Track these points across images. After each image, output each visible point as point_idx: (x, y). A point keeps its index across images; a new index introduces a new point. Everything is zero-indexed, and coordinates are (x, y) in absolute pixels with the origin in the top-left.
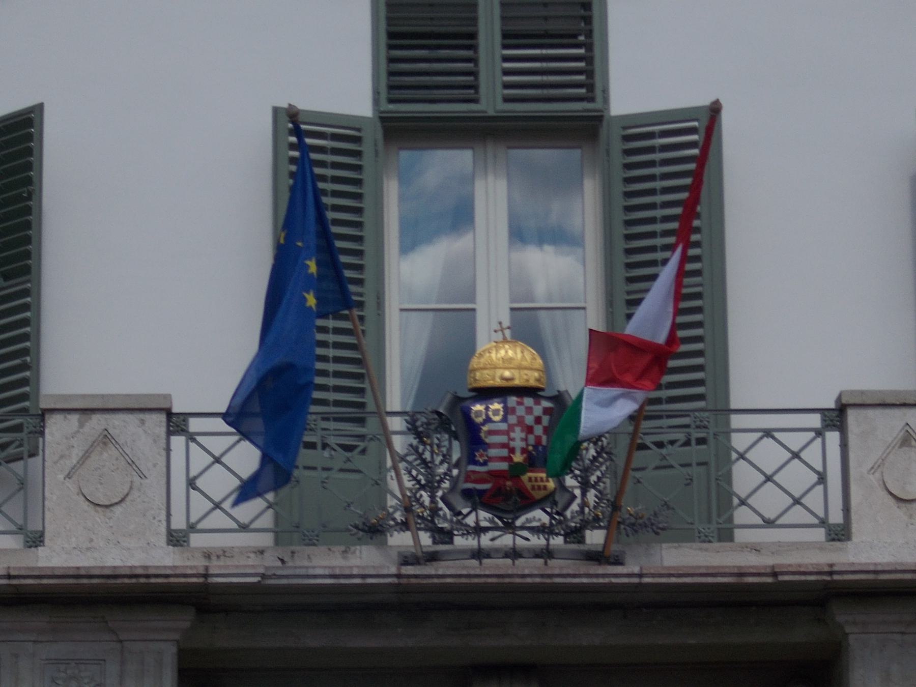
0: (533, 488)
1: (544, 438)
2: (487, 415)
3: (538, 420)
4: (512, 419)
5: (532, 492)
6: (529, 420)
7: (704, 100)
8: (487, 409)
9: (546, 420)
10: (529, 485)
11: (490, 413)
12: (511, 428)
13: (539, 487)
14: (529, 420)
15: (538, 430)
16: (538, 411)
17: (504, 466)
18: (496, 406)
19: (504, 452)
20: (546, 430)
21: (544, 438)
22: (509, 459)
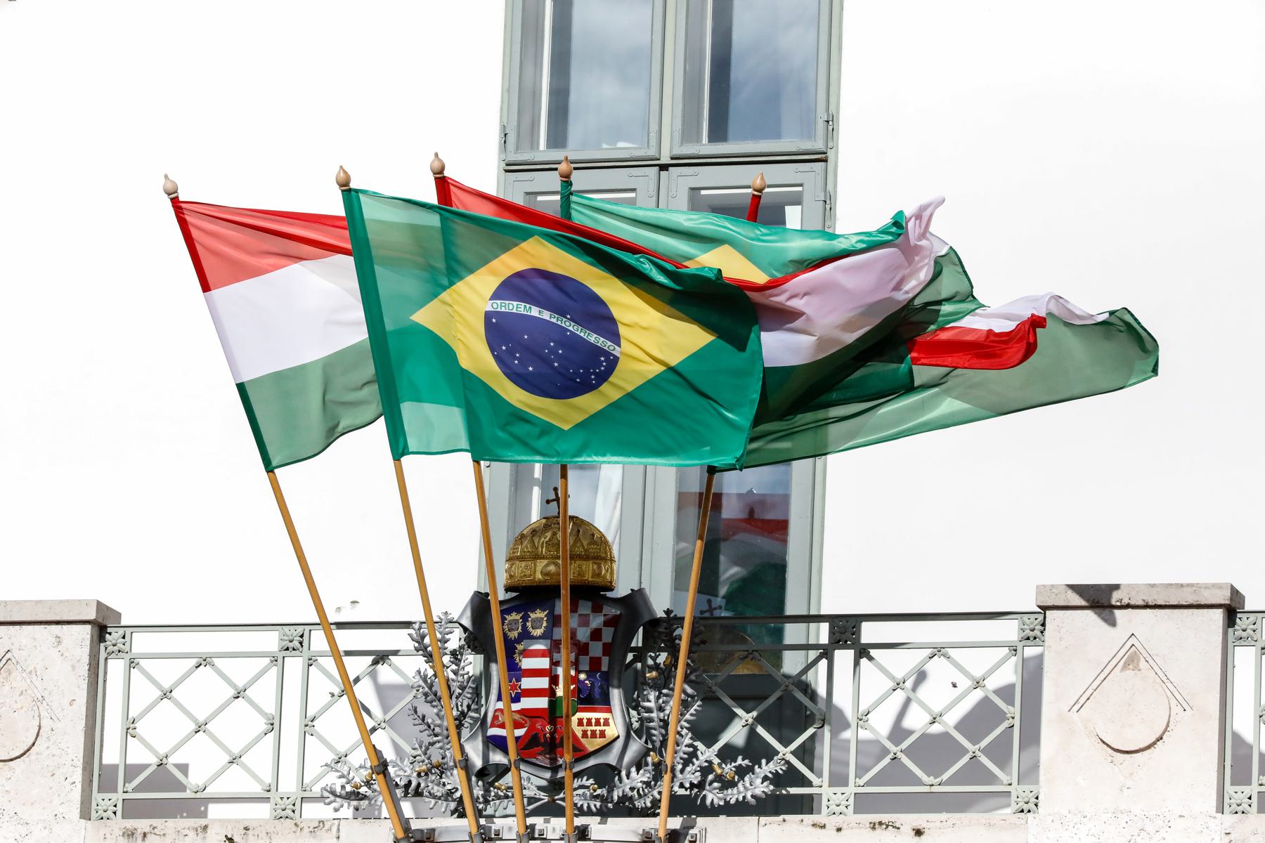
0: (585, 734)
1: (605, 660)
2: (524, 627)
3: (596, 635)
4: (560, 633)
5: (583, 741)
6: (583, 635)
7: (887, 219)
8: (525, 619)
9: (608, 634)
10: (578, 731)
11: (529, 624)
12: (556, 645)
13: (594, 734)
14: (583, 635)
15: (596, 649)
16: (597, 621)
17: (542, 703)
18: (539, 614)
19: (543, 683)
20: (607, 649)
21: (605, 660)
22: (551, 693)
